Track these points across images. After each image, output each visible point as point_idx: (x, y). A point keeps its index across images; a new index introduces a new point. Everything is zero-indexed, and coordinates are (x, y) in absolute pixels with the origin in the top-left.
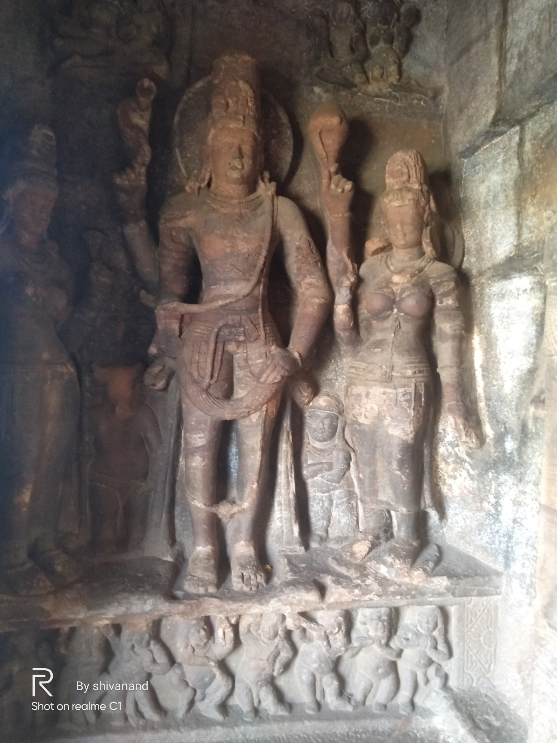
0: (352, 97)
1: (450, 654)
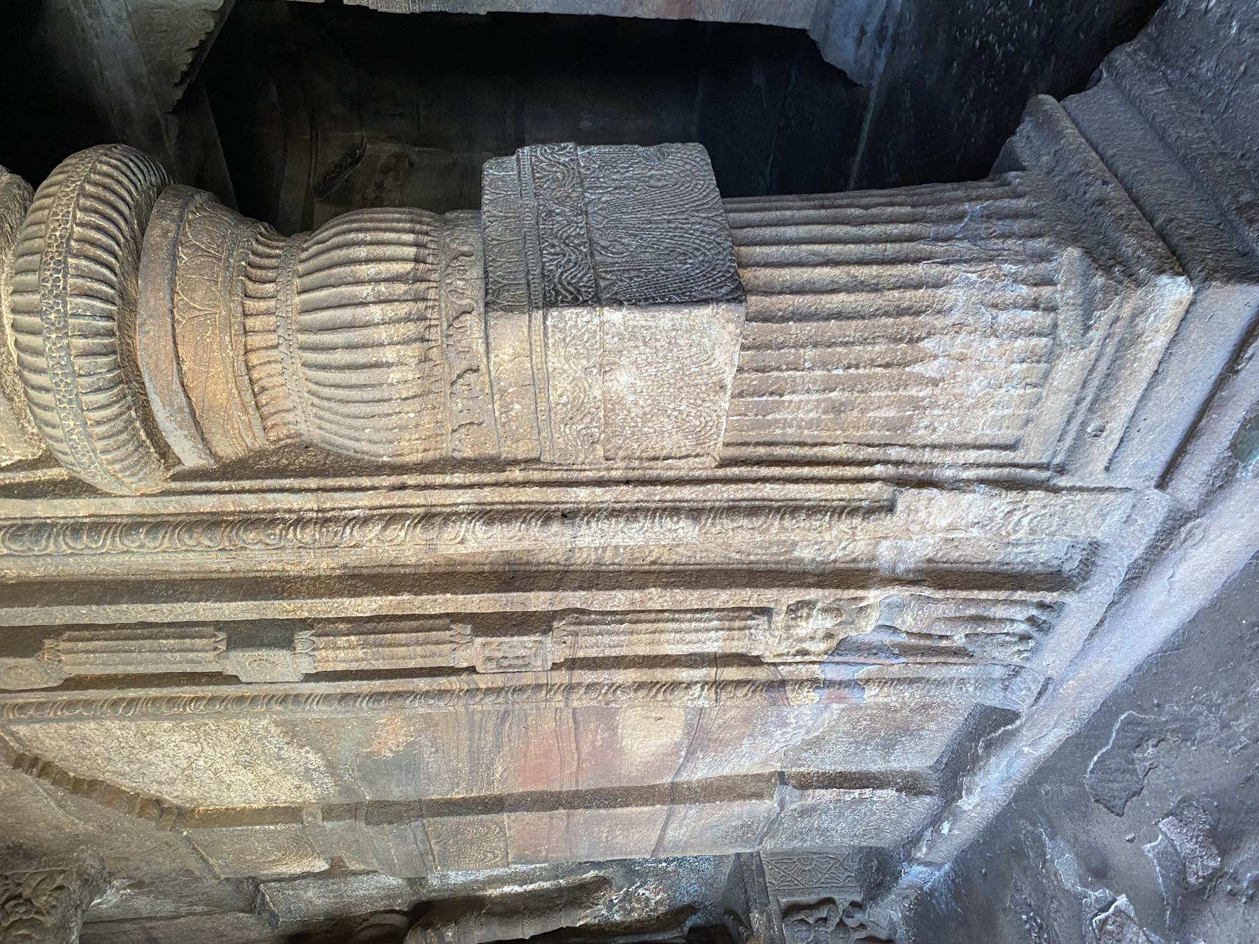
1: (830, 901)
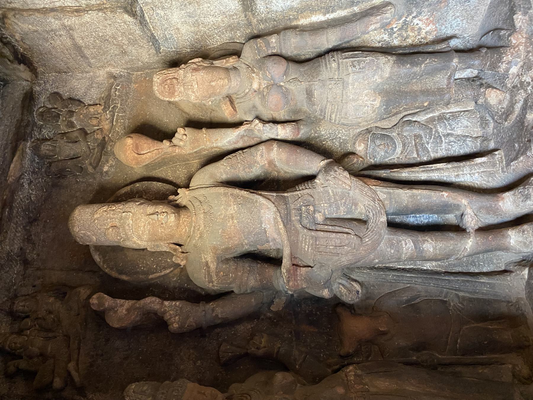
0: (112, 141)
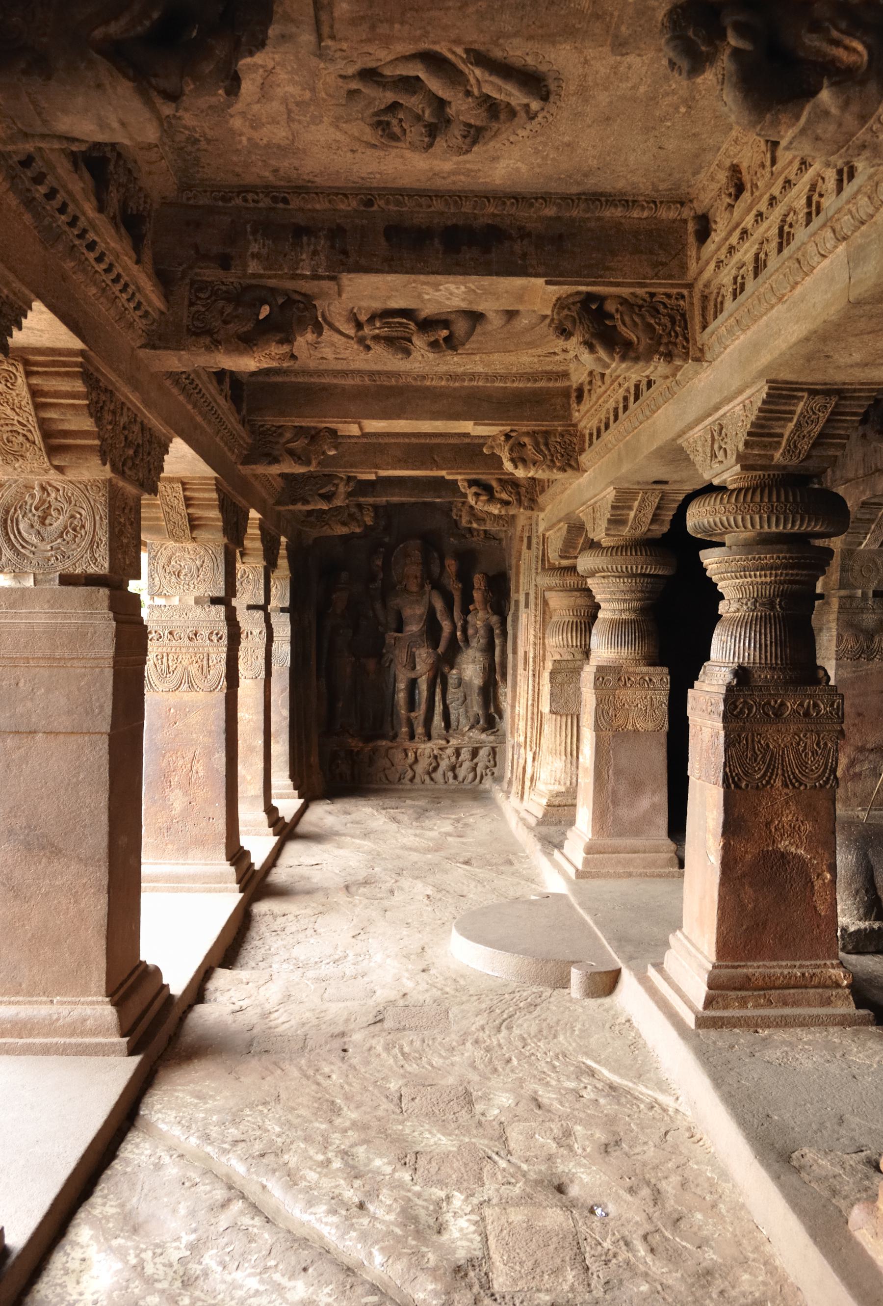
1: (495, 765)
